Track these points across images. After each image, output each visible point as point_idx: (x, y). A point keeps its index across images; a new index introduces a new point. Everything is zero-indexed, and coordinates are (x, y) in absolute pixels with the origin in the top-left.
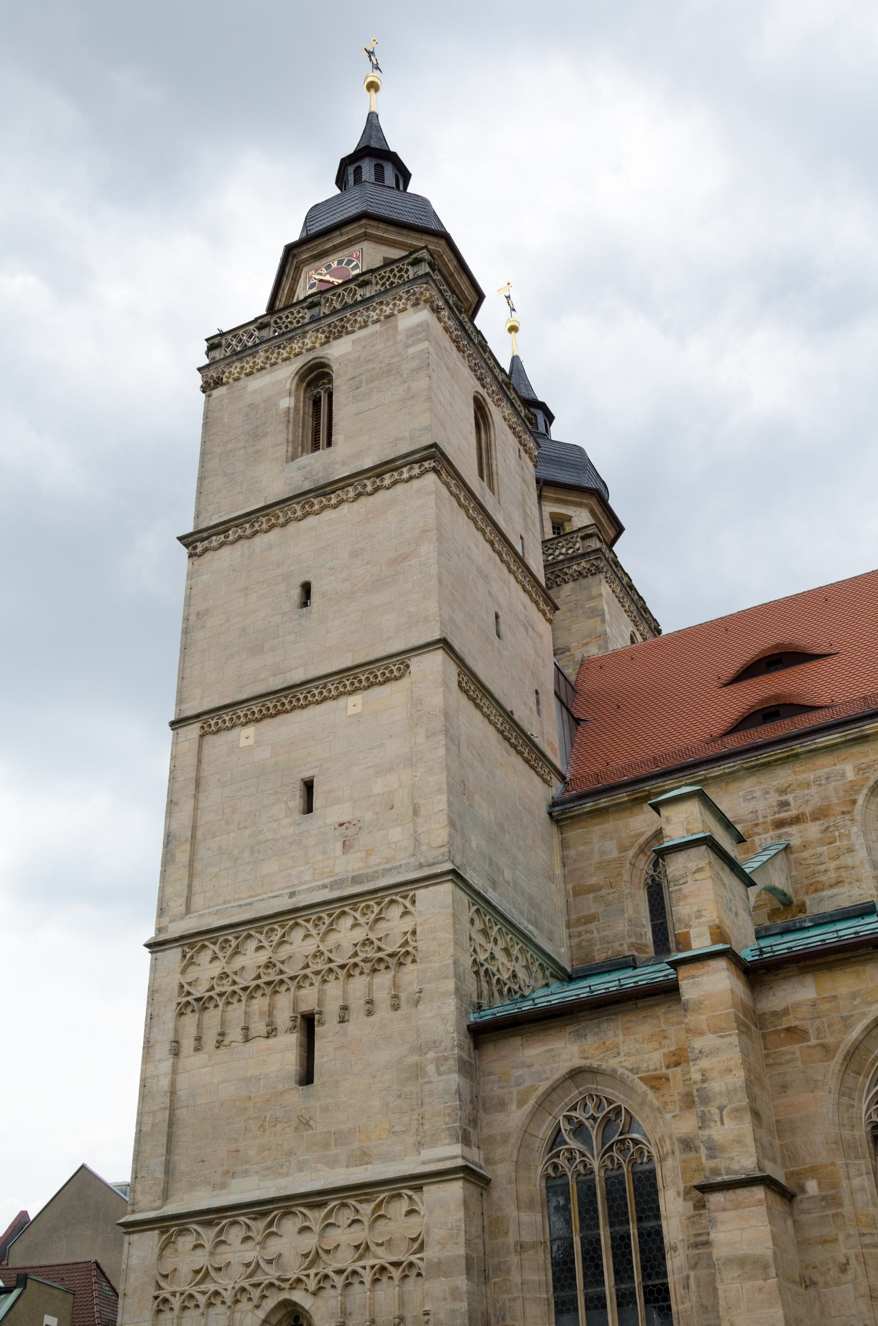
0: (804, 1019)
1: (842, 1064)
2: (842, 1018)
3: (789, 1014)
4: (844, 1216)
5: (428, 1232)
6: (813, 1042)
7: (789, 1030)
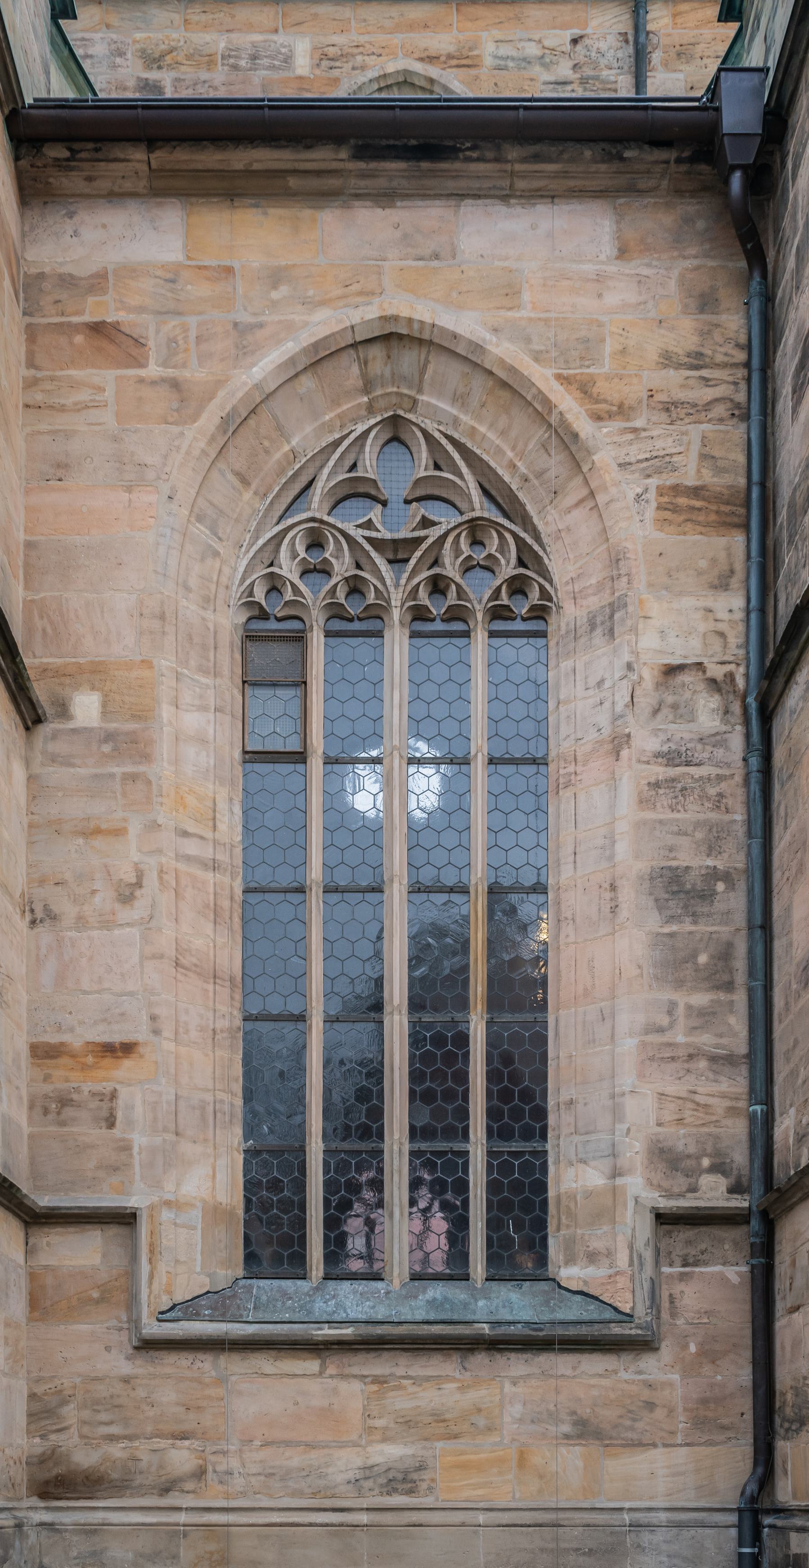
0: (141, 309)
1: (213, 439)
2: (236, 325)
3: (104, 291)
4: (149, 783)
6: (153, 370)
7: (97, 329)
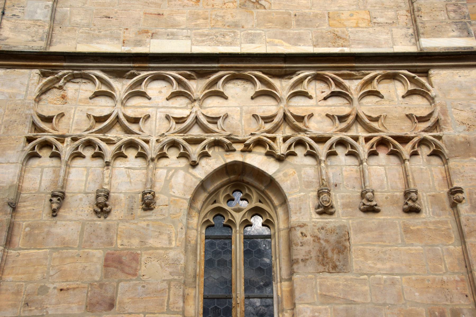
5: (444, 112)
